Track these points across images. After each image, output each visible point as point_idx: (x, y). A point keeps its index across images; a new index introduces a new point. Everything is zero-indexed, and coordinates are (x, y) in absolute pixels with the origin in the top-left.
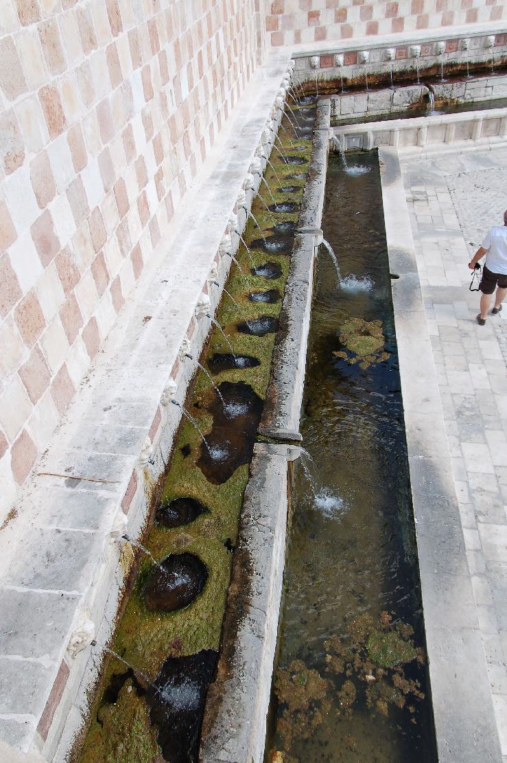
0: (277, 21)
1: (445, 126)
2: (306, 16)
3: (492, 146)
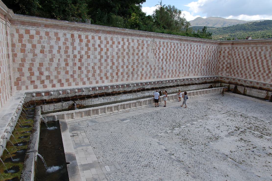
0: (19, 83)
1: (81, 113)
2: (30, 82)
3: (96, 117)
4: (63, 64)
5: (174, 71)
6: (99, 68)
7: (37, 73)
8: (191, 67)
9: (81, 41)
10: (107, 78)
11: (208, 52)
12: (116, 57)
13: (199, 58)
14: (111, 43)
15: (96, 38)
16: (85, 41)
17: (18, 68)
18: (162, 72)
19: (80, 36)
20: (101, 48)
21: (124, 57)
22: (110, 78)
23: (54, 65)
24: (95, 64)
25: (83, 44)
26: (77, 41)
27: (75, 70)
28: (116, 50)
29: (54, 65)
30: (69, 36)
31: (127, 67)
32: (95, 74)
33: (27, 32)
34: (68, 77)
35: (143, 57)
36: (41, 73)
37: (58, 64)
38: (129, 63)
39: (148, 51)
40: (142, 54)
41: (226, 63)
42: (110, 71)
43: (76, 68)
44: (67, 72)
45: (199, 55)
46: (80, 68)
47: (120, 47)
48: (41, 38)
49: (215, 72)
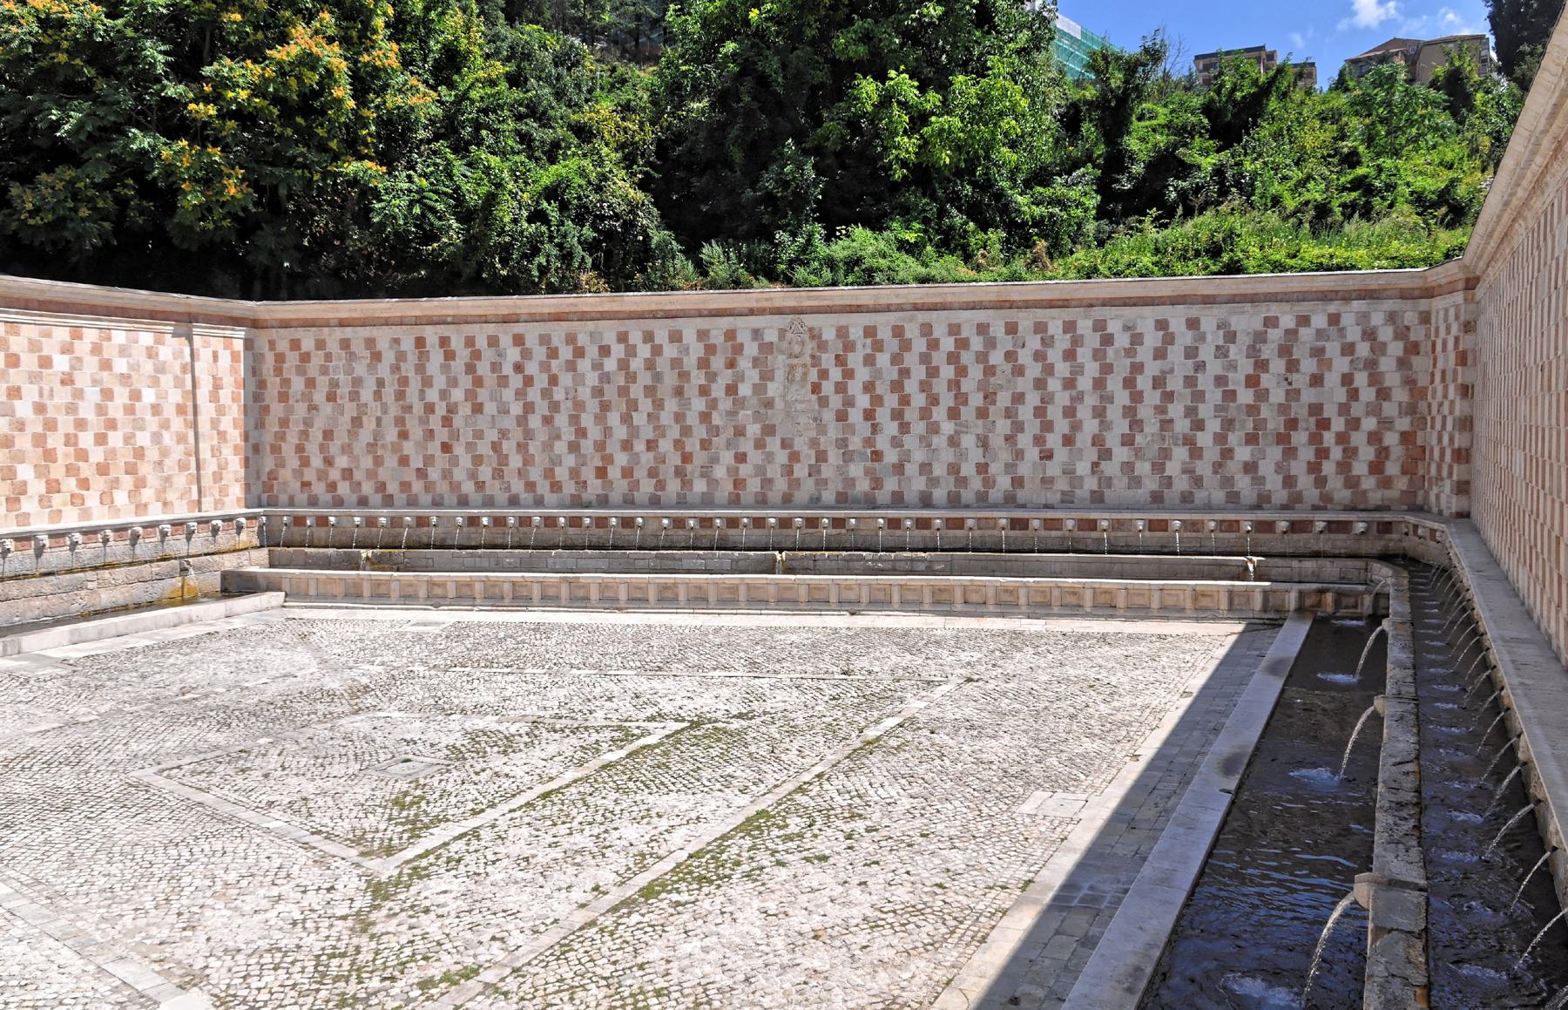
0: (272, 486)
2: (298, 485)
4: (391, 435)
5: (968, 470)
6: (522, 447)
7: (317, 462)
8: (1121, 454)
9: (450, 355)
10: (556, 487)
11: (1285, 351)
12: (592, 405)
13: (1199, 396)
14: (566, 353)
15: (506, 341)
16: (463, 354)
17: (272, 446)
18: (867, 472)
19: (444, 342)
20: (525, 377)
21: (633, 405)
22: (569, 488)
23: (366, 435)
24: (504, 434)
25: (458, 366)
26: (436, 357)
27: (429, 452)
28: (592, 379)
29: (366, 435)
30: (408, 345)
31: (651, 445)
32: (502, 471)
33: (295, 345)
34: (409, 475)
35: (740, 403)
36: (329, 462)
37: (377, 436)
38: (661, 431)
39: (767, 376)
40: (731, 390)
41: (1449, 426)
42: (570, 461)
43: (434, 448)
44: (404, 461)
45: (1190, 381)
46: (446, 448)
47: (610, 365)
48: (328, 357)
49: (1402, 484)
